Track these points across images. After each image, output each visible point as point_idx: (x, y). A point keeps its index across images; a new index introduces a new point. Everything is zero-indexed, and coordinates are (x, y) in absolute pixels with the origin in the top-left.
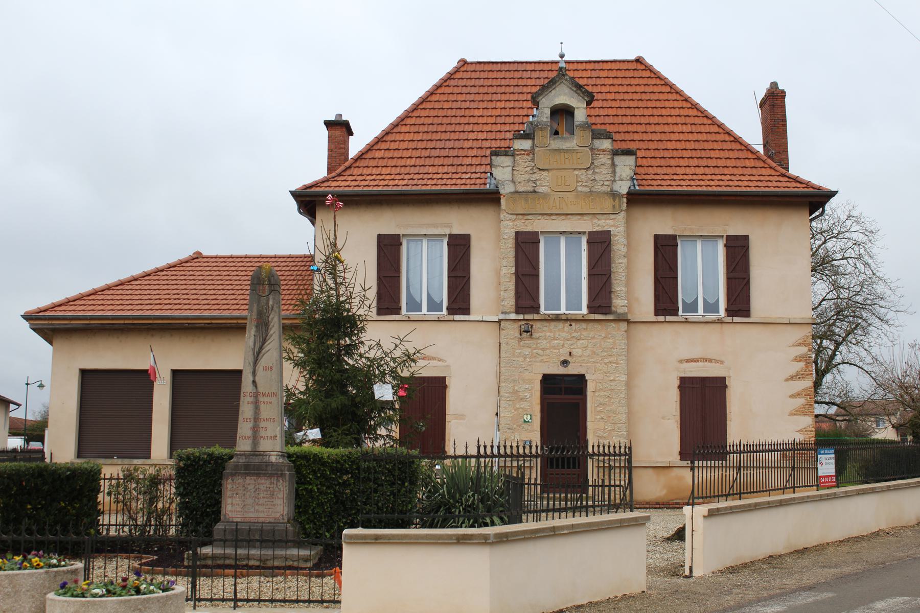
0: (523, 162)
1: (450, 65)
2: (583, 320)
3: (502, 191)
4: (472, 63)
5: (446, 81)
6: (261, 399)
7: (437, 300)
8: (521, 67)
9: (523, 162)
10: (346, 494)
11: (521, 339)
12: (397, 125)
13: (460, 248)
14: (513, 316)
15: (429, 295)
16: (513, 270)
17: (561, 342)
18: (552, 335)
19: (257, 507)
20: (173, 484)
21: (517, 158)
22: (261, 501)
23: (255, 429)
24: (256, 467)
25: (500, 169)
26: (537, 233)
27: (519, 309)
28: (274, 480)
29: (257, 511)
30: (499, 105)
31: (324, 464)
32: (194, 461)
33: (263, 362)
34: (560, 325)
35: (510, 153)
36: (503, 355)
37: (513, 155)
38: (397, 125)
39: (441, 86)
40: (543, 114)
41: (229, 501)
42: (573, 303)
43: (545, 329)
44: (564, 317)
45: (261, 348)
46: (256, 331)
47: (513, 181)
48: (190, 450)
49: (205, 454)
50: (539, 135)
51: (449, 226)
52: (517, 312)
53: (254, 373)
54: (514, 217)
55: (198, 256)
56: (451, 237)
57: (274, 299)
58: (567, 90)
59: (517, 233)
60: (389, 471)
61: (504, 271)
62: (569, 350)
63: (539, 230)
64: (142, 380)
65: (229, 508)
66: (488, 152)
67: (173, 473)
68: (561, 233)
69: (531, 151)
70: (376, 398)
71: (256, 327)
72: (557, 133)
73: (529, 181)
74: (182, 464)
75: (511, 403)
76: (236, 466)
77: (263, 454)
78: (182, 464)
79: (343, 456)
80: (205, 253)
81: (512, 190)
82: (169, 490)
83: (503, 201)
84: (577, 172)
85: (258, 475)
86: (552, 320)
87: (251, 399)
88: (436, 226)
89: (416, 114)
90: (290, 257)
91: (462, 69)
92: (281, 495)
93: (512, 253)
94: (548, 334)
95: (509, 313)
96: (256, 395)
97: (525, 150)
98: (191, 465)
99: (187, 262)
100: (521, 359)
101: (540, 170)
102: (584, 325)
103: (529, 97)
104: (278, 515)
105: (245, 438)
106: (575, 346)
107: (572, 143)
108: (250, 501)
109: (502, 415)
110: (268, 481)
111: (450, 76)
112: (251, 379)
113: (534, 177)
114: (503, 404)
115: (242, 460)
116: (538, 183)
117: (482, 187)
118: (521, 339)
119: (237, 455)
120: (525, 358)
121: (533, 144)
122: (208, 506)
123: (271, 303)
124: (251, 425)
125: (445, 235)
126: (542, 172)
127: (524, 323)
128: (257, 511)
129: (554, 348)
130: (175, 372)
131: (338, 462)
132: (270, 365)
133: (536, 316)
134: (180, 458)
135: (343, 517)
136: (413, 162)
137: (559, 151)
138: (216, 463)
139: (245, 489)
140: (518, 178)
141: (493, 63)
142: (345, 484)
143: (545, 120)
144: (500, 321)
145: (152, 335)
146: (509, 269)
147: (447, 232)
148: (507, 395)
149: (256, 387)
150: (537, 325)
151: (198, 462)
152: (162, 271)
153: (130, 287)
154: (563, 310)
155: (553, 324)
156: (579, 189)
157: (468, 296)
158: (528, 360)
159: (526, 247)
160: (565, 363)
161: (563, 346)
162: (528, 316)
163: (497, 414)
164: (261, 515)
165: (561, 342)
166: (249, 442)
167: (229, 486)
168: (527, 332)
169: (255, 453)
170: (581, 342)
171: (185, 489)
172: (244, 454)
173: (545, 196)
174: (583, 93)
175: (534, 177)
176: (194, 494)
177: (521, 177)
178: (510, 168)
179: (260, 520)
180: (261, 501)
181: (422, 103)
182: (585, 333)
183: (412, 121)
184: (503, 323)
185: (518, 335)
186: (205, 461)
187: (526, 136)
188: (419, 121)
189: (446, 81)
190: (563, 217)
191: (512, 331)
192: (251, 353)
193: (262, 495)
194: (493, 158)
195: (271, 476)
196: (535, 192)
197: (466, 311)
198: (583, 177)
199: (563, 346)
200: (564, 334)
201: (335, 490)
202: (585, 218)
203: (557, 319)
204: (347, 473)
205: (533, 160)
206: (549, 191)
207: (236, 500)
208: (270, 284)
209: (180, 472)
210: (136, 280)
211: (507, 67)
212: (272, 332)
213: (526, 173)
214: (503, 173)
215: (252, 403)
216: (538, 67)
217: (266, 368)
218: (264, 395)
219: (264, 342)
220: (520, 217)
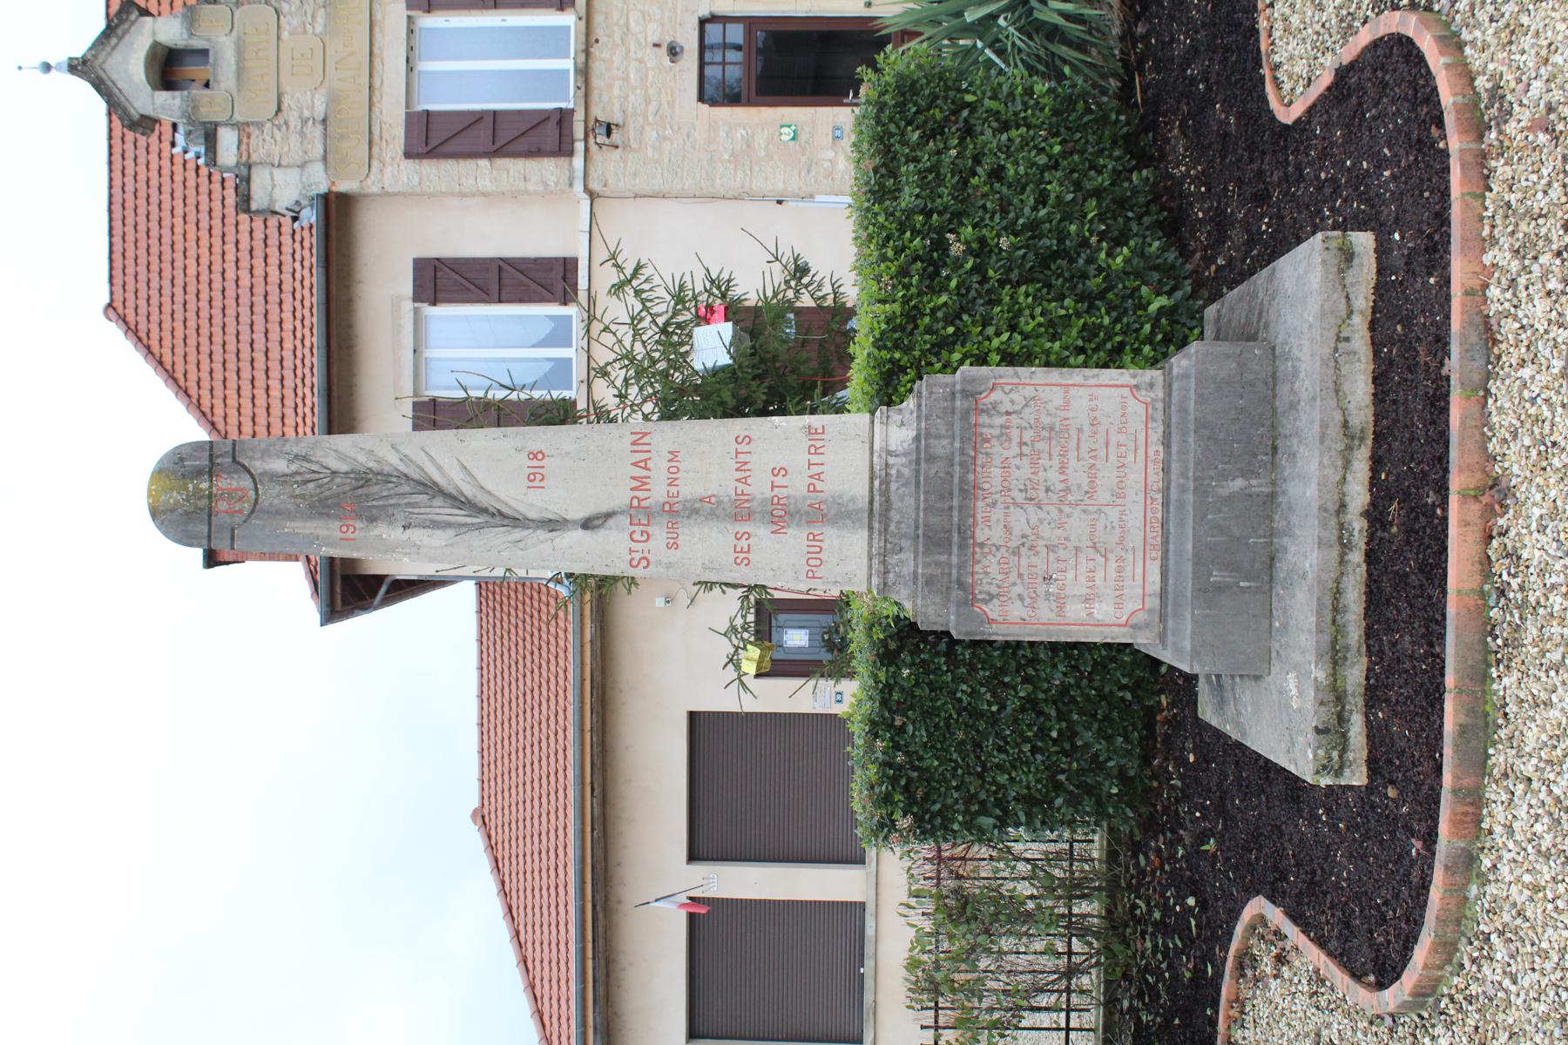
0: (263, 145)
1: (114, 331)
2: (588, 19)
3: (323, 189)
4: (112, 293)
5: (140, 339)
6: (658, 493)
7: (548, 327)
8: (118, 199)
9: (263, 145)
10: (1014, 247)
11: (627, 147)
12: (213, 424)
13: (441, 280)
14: (578, 161)
15: (542, 344)
16: (483, 163)
17: (633, 64)
18: (617, 84)
19: (1103, 496)
20: (959, 850)
21: (254, 158)
22: (1077, 477)
23: (780, 514)
24: (936, 510)
25: (277, 193)
26: (408, 115)
27: (563, 149)
28: (990, 425)
29: (1119, 494)
30: (231, 274)
31: (912, 315)
32: (894, 781)
33: (510, 492)
34: (597, 67)
35: (244, 171)
36: (657, 184)
37: (250, 167)
38: (213, 424)
39: (148, 348)
40: (167, 105)
41: (1075, 611)
42: (549, 42)
43: (605, 98)
44: (582, 58)
46: (390, 518)
47: (303, 166)
48: (859, 801)
49: (870, 748)
50: (208, 113)
51: (396, 302)
52: (570, 153)
53: (553, 525)
54: (375, 163)
55: (482, 818)
56: (417, 298)
57: (265, 454)
58: (117, 56)
59: (408, 155)
60: (926, 138)
61: (485, 183)
62: (650, 49)
63: (403, 111)
64: (708, 924)
65: (1104, 611)
66: (244, 217)
67: (926, 849)
68: (410, 69)
69: (242, 128)
70: (725, 360)
71: (372, 519)
72: (207, 85)
73: (302, 134)
74: (1163, 670)
75: (756, 168)
77: (881, 481)
78: (904, 823)
79: (884, 258)
80: (476, 804)
81: (319, 166)
82: (982, 864)
83: (343, 187)
84: (285, 35)
85: (969, 491)
86: (587, 82)
87: (659, 532)
89: (193, 391)
91: (120, 311)
92: (1055, 397)
93: (450, 166)
94: (616, 91)
95: (571, 170)
96: (640, 514)
97: (240, 142)
98: (906, 789)
99: (489, 837)
100: (667, 146)
101: (279, 110)
102: (598, 19)
103: (130, 136)
104: (1136, 409)
105: (815, 556)
106: (641, 38)
107: (225, 48)
108: (1077, 527)
109: (780, 186)
110: (996, 448)
111: (132, 331)
112: (579, 533)
113: (294, 122)
114: (758, 184)
115: (906, 562)
116: (307, 114)
117: (314, 231)
118: (627, 147)
120: (665, 139)
121: (226, 124)
122: (1043, 733)
123: (280, 466)
124: (761, 534)
125: (416, 310)
126: (285, 106)
127: (591, 140)
128: (1119, 494)
129: (644, 79)
130: (693, 857)
131: (903, 272)
132: (523, 460)
133: (579, 116)
134: (885, 828)
135: (1091, 260)
136: (275, 384)
137: (240, 72)
138: (901, 708)
139: (1027, 544)
140: (298, 157)
141: (111, 252)
142: (982, 250)
143: (178, 102)
144: (593, 196)
145: (619, 902)
146: (482, 173)
147: (408, 305)
148: (740, 175)
149: (609, 515)
150: (598, 112)
151: (900, 767)
152: (503, 883)
153: (529, 945)
154: (568, 64)
155: (595, 82)
156: (319, 29)
157: (536, 260)
158: (668, 132)
159: (435, 137)
160: (674, 52)
161: (640, 61)
162: (579, 131)
163: (780, 202)
164: (1135, 477)
165: (633, 64)
166: (831, 537)
167: (1017, 611)
168: (609, 133)
169: (878, 514)
170: (632, 24)
171: (984, 811)
172: (882, 558)
173: (333, 100)
174: (121, 21)
175: (294, 122)
176: (1003, 779)
177: (293, 148)
178: (277, 172)
179: (1156, 478)
180: (1077, 477)
181: (175, 380)
182: (615, 16)
183: (205, 393)
184: (595, 186)
185: (617, 154)
186: (896, 747)
187: (210, 138)
188: (206, 384)
189: (140, 339)
190: (377, 62)
191: (608, 166)
192: (476, 540)
193: (1053, 476)
194: (254, 207)
195: (972, 439)
196: (324, 121)
197: (568, 266)
198: (296, 21)
199: (640, 61)
200: (617, 60)
201: (1002, 283)
202: (378, 16)
203: (584, 72)
204: (941, 245)
205: (260, 125)
206: (323, 90)
207: (1074, 582)
208: (211, 472)
209: (930, 825)
210: (518, 933)
211: (118, 224)
212: (393, 459)
213: (286, 139)
214: (286, 186)
215: (672, 528)
216: (117, 166)
217: (535, 478)
218: (642, 483)
219: (431, 488)
220: (375, 150)
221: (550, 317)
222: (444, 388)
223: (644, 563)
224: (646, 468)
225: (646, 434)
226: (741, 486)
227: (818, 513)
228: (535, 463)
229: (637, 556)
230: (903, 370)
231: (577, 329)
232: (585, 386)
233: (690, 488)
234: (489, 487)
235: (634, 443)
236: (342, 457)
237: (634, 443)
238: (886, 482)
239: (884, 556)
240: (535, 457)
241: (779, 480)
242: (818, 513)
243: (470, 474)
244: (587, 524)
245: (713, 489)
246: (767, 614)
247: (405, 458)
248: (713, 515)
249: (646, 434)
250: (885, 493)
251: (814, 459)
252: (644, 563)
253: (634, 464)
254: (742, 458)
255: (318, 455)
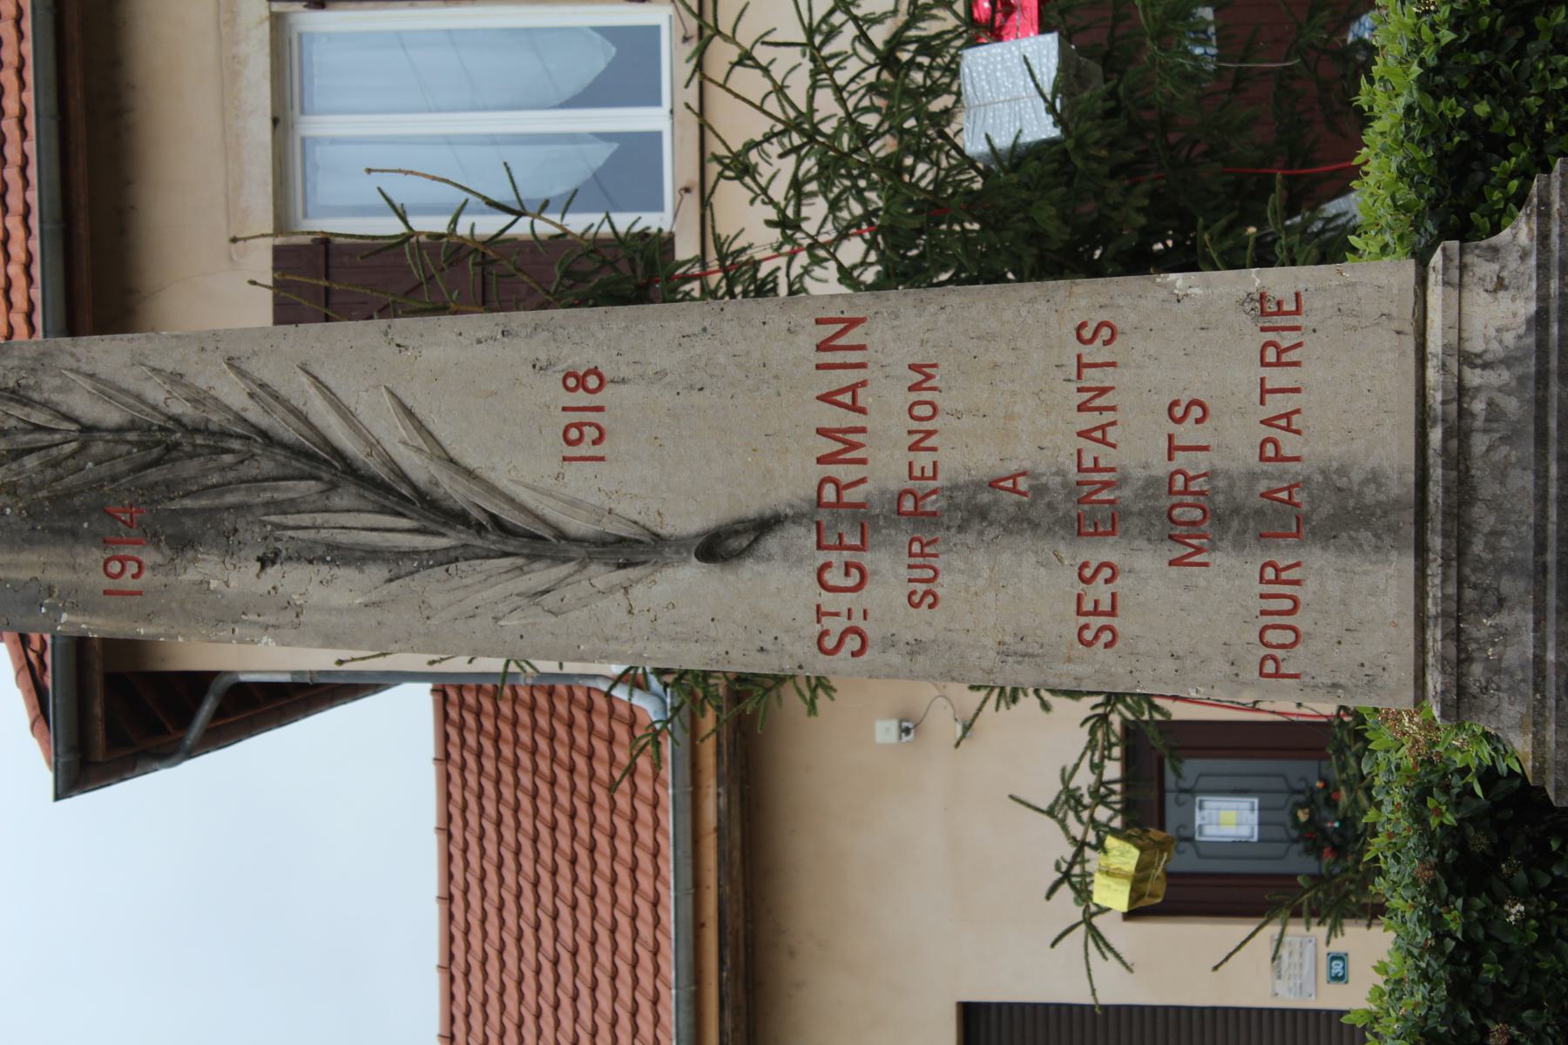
6: (885, 468)
7: (599, 59)
23: (1192, 517)
33: (521, 467)
45: (390, 492)
46: (228, 543)
53: (631, 550)
70: (1042, 128)
71: (183, 544)
76: (1567, 690)
77: (1447, 428)
87: (889, 567)
88: (229, 70)
90: (446, 832)
105: (1280, 626)
112: (690, 574)
115: (1515, 635)
119: (1459, 703)
124: (1145, 568)
125: (278, 23)
132: (552, 391)
149: (765, 525)
166: (1321, 572)
169: (1438, 513)
172: (1452, 630)
192: (432, 585)
212: (233, 394)
217: (582, 436)
218: (844, 445)
221: (608, 32)
222: (346, 210)
223: (853, 643)
224: (854, 408)
225: (853, 323)
226: (1091, 449)
227: (1283, 514)
228: (581, 399)
229: (836, 626)
230: (1500, 147)
231: (672, 62)
232: (693, 200)
233: (964, 455)
234: (471, 460)
235: (823, 347)
236: (106, 390)
237: (823, 347)
238: (1459, 431)
239: (1457, 617)
240: (581, 383)
241: (1187, 433)
242: (1283, 514)
243: (421, 427)
244: (714, 548)
245: (1022, 455)
246: (1150, 763)
247: (263, 392)
248: (1022, 522)
249: (853, 323)
250: (1458, 460)
251: (1277, 377)
252: (853, 643)
253: (826, 398)
254: (1093, 377)
255: (48, 386)
